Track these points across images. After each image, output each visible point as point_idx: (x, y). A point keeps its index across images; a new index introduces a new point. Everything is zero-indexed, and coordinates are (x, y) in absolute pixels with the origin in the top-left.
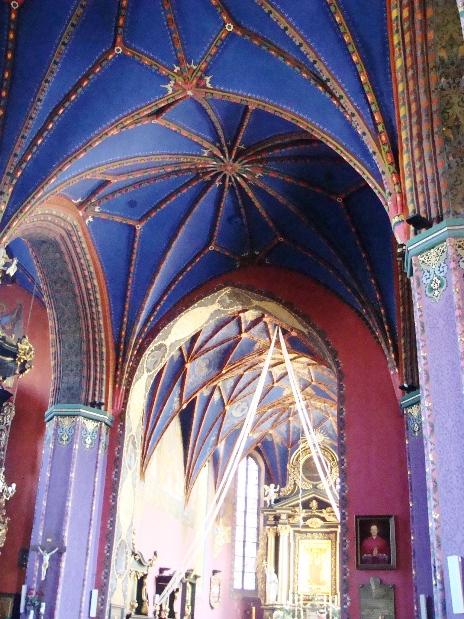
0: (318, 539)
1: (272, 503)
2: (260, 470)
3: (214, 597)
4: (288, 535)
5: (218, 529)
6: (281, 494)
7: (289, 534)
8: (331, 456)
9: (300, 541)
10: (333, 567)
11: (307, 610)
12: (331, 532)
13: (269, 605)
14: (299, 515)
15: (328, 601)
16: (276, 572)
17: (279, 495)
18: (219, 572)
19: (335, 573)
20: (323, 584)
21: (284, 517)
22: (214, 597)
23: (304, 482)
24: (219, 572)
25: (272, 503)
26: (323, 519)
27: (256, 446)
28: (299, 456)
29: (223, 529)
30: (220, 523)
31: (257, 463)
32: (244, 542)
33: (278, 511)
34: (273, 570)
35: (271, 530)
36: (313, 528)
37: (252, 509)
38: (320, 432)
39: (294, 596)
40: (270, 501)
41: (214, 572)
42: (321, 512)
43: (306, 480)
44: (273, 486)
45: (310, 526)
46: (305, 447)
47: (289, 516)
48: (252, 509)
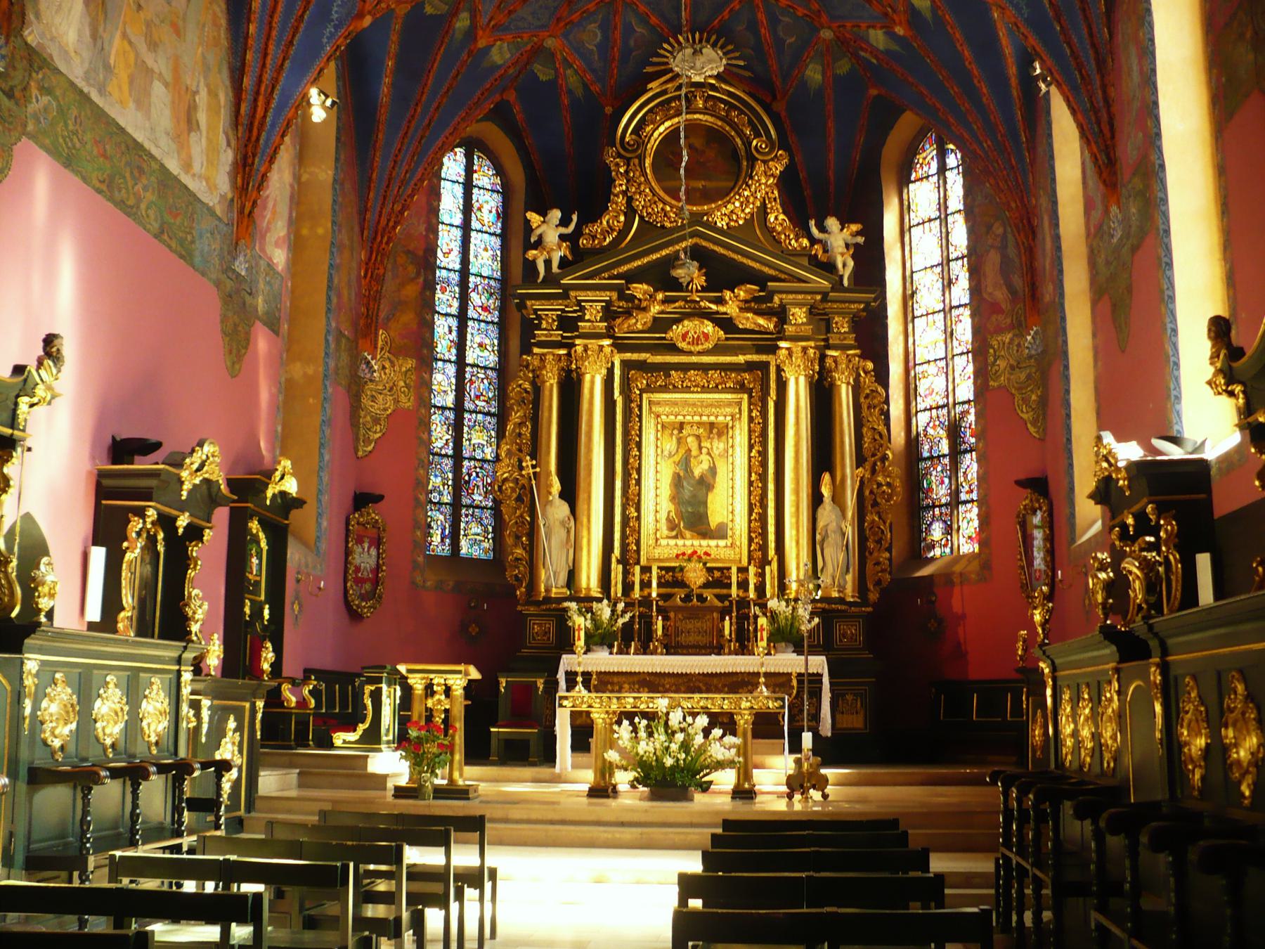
0: (705, 389)
1: (555, 269)
2: (506, 192)
3: (359, 581)
4: (604, 372)
5: (373, 362)
6: (583, 242)
7: (610, 372)
8: (751, 122)
9: (645, 396)
10: (754, 477)
11: (672, 615)
12: (750, 367)
13: (548, 600)
14: (645, 309)
15: (743, 585)
16: (570, 494)
17: (575, 248)
18: (379, 498)
19: (764, 496)
20: (720, 533)
21: (593, 312)
22: (359, 581)
23: (661, 206)
24: (379, 498)
25: (555, 269)
26: (725, 324)
27: (497, 98)
28: (642, 123)
29: (387, 365)
30: (380, 343)
31: (499, 170)
32: (459, 408)
33: (572, 294)
34: (556, 486)
35: (550, 357)
36: (690, 353)
37: (485, 309)
38: (714, 46)
39: (626, 573)
40: (548, 263)
41: (362, 500)
42: (720, 301)
43: (667, 198)
44: (556, 215)
45: (682, 345)
46: (664, 92)
47: (609, 313)
48: (485, 309)
